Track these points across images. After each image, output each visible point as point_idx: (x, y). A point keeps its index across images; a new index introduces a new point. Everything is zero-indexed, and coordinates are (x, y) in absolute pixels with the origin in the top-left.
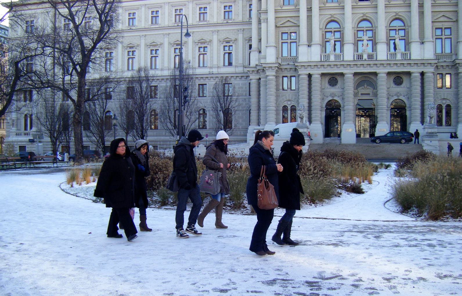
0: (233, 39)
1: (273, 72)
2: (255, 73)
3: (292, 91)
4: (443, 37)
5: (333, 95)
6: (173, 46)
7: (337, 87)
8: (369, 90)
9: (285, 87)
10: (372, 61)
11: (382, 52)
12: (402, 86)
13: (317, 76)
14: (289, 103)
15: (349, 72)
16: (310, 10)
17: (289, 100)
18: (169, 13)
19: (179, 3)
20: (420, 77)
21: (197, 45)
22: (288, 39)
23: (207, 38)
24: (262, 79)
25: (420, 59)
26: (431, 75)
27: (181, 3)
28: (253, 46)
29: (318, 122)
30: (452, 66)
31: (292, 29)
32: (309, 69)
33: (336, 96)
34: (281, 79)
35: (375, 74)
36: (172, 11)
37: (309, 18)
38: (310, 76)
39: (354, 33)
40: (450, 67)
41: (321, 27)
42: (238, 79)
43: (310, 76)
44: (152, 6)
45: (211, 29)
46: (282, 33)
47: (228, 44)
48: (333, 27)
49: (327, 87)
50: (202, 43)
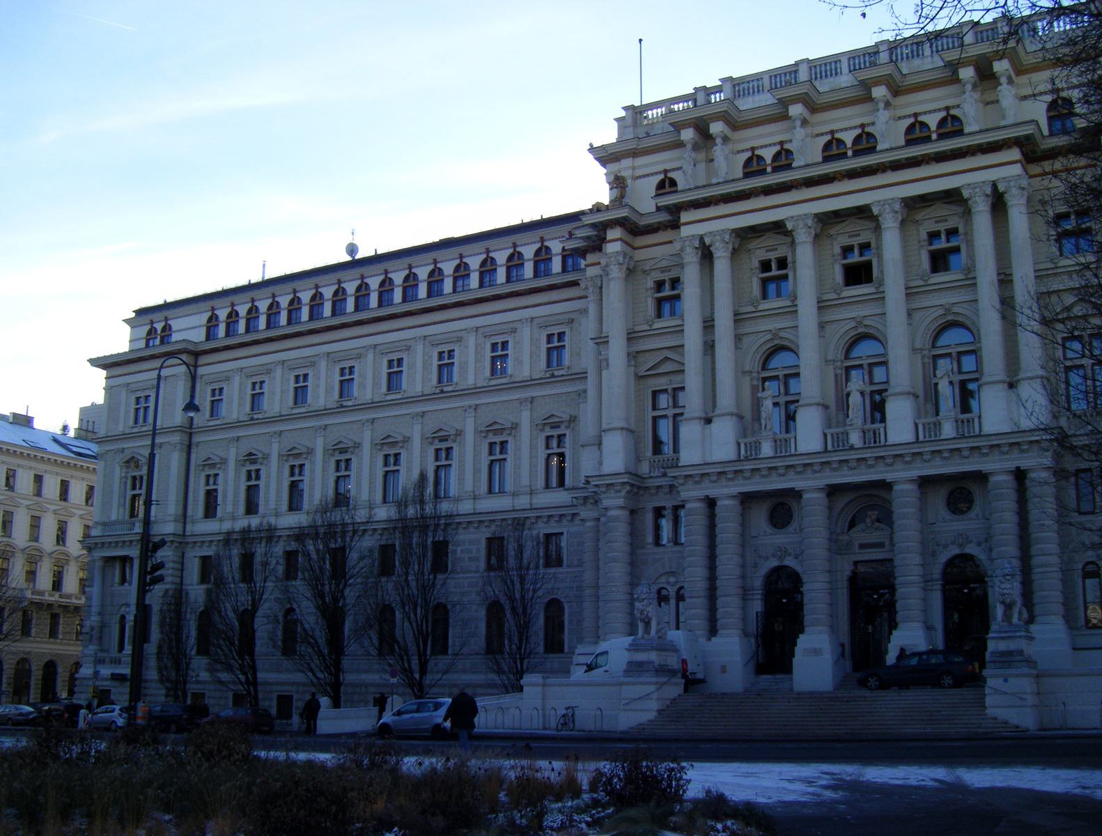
0: (566, 417)
1: (619, 497)
2: (591, 503)
3: (677, 548)
5: (782, 552)
6: (431, 444)
9: (665, 541)
10: (869, 450)
13: (726, 502)
14: (672, 580)
15: (810, 485)
16: (708, 325)
17: (672, 573)
19: (446, 335)
25: (1009, 431)
27: (451, 335)
29: (730, 631)
33: (790, 555)
34: (649, 517)
35: (886, 486)
36: (431, 357)
37: (709, 347)
39: (836, 375)
43: (711, 503)
44: (387, 349)
45: (517, 396)
49: (765, 532)
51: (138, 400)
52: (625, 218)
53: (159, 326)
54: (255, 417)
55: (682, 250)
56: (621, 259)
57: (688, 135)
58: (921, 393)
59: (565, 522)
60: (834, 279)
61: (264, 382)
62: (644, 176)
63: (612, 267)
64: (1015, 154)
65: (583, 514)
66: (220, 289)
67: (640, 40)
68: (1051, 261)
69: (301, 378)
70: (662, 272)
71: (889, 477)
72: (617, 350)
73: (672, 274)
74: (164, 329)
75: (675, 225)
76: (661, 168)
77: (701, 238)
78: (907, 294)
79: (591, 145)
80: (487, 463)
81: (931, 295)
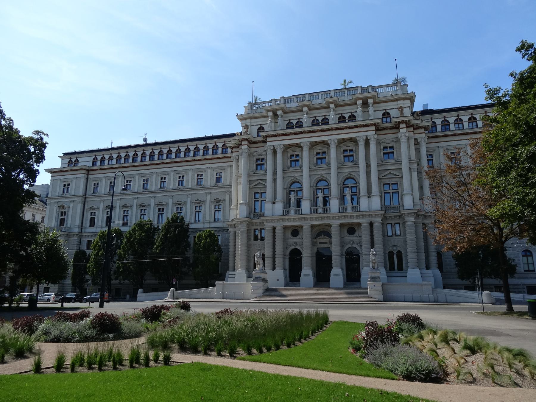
4: (391, 191)
12: (355, 235)
15: (306, 225)
16: (275, 173)
18: (174, 179)
20: (369, 227)
23: (201, 199)
30: (400, 216)
37: (275, 180)
38: (274, 229)
39: (313, 191)
40: (398, 217)
41: (285, 187)
42: (224, 232)
46: (255, 193)
47: (218, 204)
50: (198, 203)
51: (65, 185)
52: (249, 138)
53: (73, 160)
55: (267, 149)
56: (247, 151)
57: (270, 114)
58: (312, 200)
59: (220, 232)
60: (314, 162)
61: (131, 180)
62: (254, 125)
63: (244, 153)
66: (97, 149)
67: (253, 82)
68: (381, 161)
69: (129, 181)
70: (259, 156)
73: (262, 157)
74: (75, 161)
75: (265, 142)
76: (260, 123)
78: (337, 168)
79: (237, 115)
80: (195, 212)
81: (384, 166)
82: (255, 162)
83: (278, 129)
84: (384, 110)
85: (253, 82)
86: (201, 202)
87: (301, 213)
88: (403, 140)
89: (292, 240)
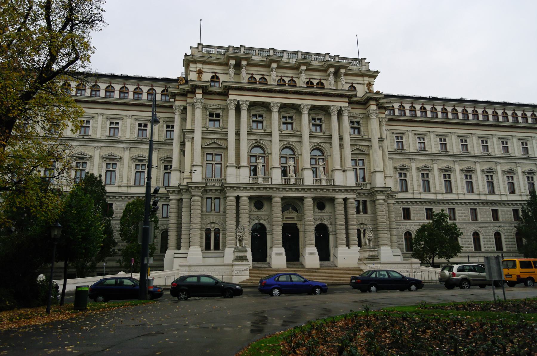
4: (358, 168)
5: (258, 218)
7: (263, 210)
8: (294, 214)
11: (308, 178)
16: (238, 134)
17: (213, 223)
21: (105, 160)
22: (212, 160)
24: (184, 200)
26: (353, 200)
28: (173, 167)
30: (368, 194)
31: (218, 151)
32: (238, 190)
35: (302, 199)
38: (238, 198)
43: (238, 198)
48: (258, 152)
54: (85, 137)
64: (346, 100)
65: (171, 197)
71: (305, 195)
72: (198, 136)
76: (214, 71)
77: (238, 101)
82: (208, 116)
83: (242, 81)
84: (350, 83)
85: (201, 20)
86: (116, 158)
87: (270, 183)
88: (374, 116)
89: (257, 213)
